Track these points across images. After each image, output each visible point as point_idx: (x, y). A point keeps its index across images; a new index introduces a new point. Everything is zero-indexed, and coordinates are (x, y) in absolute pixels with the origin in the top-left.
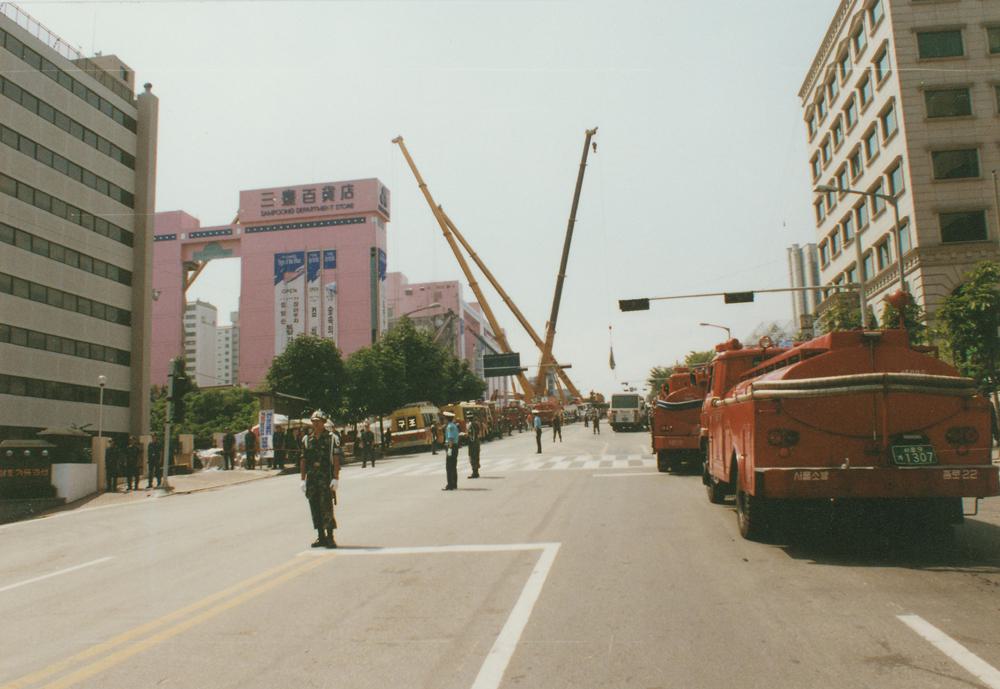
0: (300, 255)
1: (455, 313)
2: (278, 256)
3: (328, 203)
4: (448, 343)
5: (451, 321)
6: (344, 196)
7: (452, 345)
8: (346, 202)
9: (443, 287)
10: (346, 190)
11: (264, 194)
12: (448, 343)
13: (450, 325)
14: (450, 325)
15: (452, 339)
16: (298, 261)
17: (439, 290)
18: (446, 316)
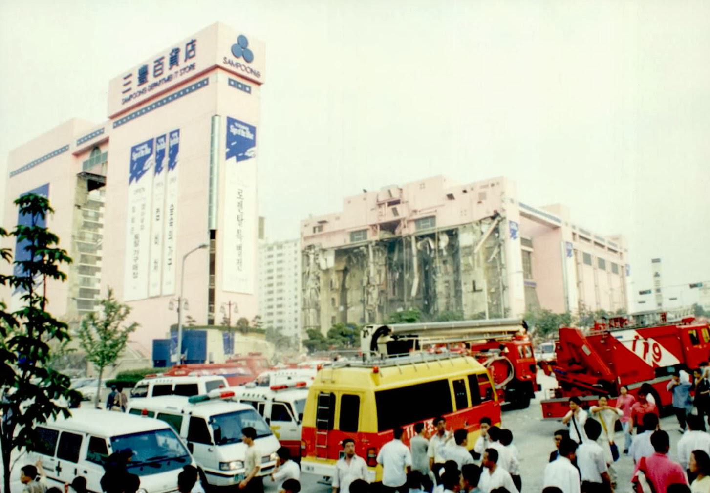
0: (150, 143)
1: (502, 214)
2: (424, 187)
3: (175, 69)
4: (496, 251)
5: (499, 221)
6: (188, 57)
7: (499, 253)
8: (190, 62)
9: (486, 186)
10: (190, 48)
11: (125, 78)
12: (496, 251)
13: (496, 230)
14: (496, 230)
15: (500, 246)
16: (148, 151)
17: (483, 190)
18: (493, 218)
